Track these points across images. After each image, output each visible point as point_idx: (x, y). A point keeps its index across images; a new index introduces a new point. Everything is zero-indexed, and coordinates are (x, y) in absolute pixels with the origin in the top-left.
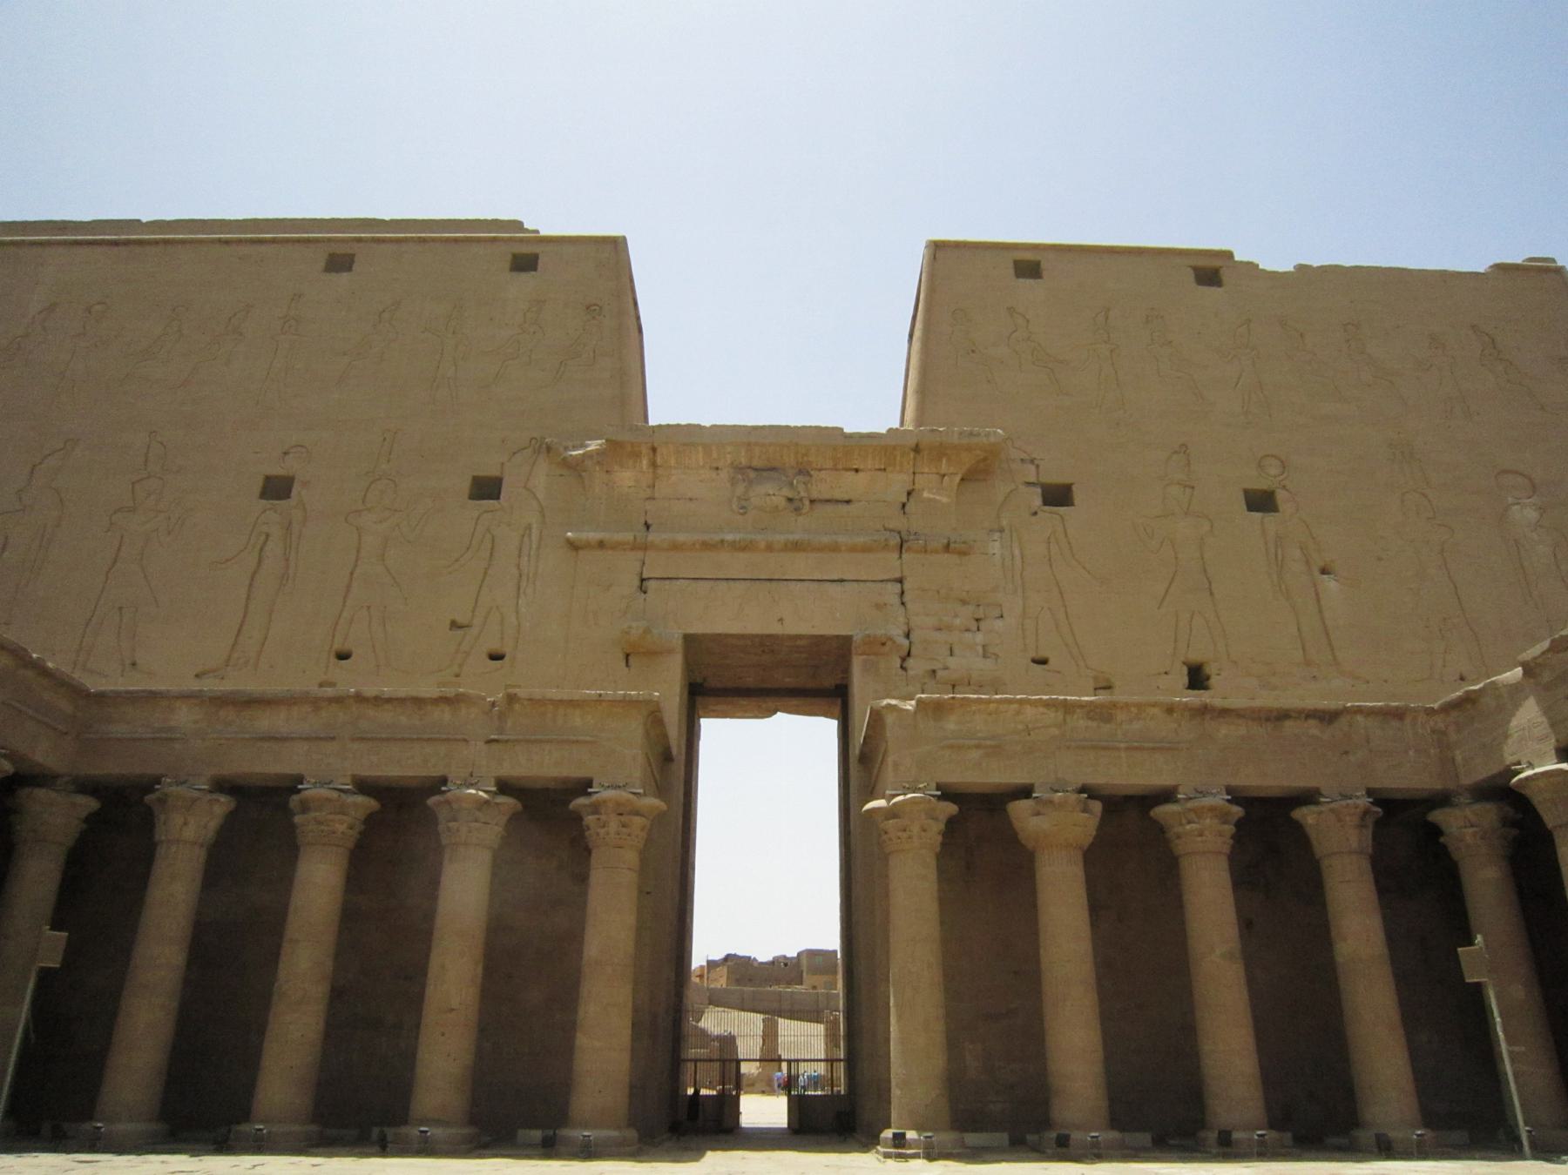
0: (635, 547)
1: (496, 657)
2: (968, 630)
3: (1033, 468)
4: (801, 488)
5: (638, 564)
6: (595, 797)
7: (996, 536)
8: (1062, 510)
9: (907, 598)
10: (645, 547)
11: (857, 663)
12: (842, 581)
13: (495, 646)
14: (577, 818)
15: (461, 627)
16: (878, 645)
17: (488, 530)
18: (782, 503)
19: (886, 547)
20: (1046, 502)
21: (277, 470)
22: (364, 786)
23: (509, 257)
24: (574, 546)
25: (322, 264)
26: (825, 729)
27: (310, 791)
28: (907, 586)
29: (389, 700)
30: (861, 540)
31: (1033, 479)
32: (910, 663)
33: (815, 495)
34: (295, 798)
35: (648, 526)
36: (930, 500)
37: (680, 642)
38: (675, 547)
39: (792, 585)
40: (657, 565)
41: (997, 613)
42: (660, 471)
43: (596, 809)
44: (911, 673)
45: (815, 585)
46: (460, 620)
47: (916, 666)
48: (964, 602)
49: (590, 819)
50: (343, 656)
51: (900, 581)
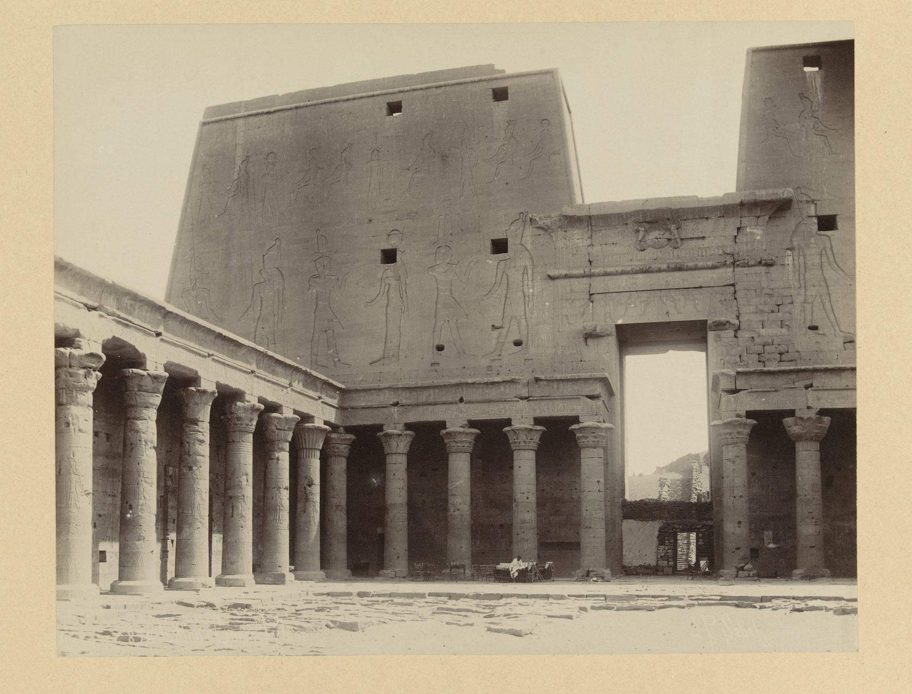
0: (583, 276)
1: (518, 343)
2: (773, 312)
3: (813, 206)
4: (675, 232)
5: (587, 286)
6: (581, 425)
7: (789, 252)
8: (829, 233)
9: (738, 295)
10: (591, 276)
11: (711, 335)
12: (701, 287)
13: (515, 337)
14: (572, 433)
15: (497, 328)
16: (720, 326)
17: (504, 272)
18: (663, 241)
19: (724, 265)
20: (820, 229)
21: (387, 247)
22: (472, 424)
23: (491, 92)
24: (552, 278)
25: (385, 111)
26: (704, 354)
27: (451, 428)
28: (737, 288)
29: (480, 384)
30: (710, 263)
31: (813, 214)
32: (740, 333)
33: (683, 237)
34: (443, 432)
35: (590, 262)
36: (751, 233)
37: (614, 329)
38: (606, 274)
39: (673, 293)
40: (598, 285)
41: (790, 301)
42: (594, 228)
43: (583, 429)
44: (741, 339)
45: (685, 291)
46: (496, 325)
47: (744, 335)
48: (771, 296)
49: (578, 435)
50: (440, 348)
51: (733, 285)
